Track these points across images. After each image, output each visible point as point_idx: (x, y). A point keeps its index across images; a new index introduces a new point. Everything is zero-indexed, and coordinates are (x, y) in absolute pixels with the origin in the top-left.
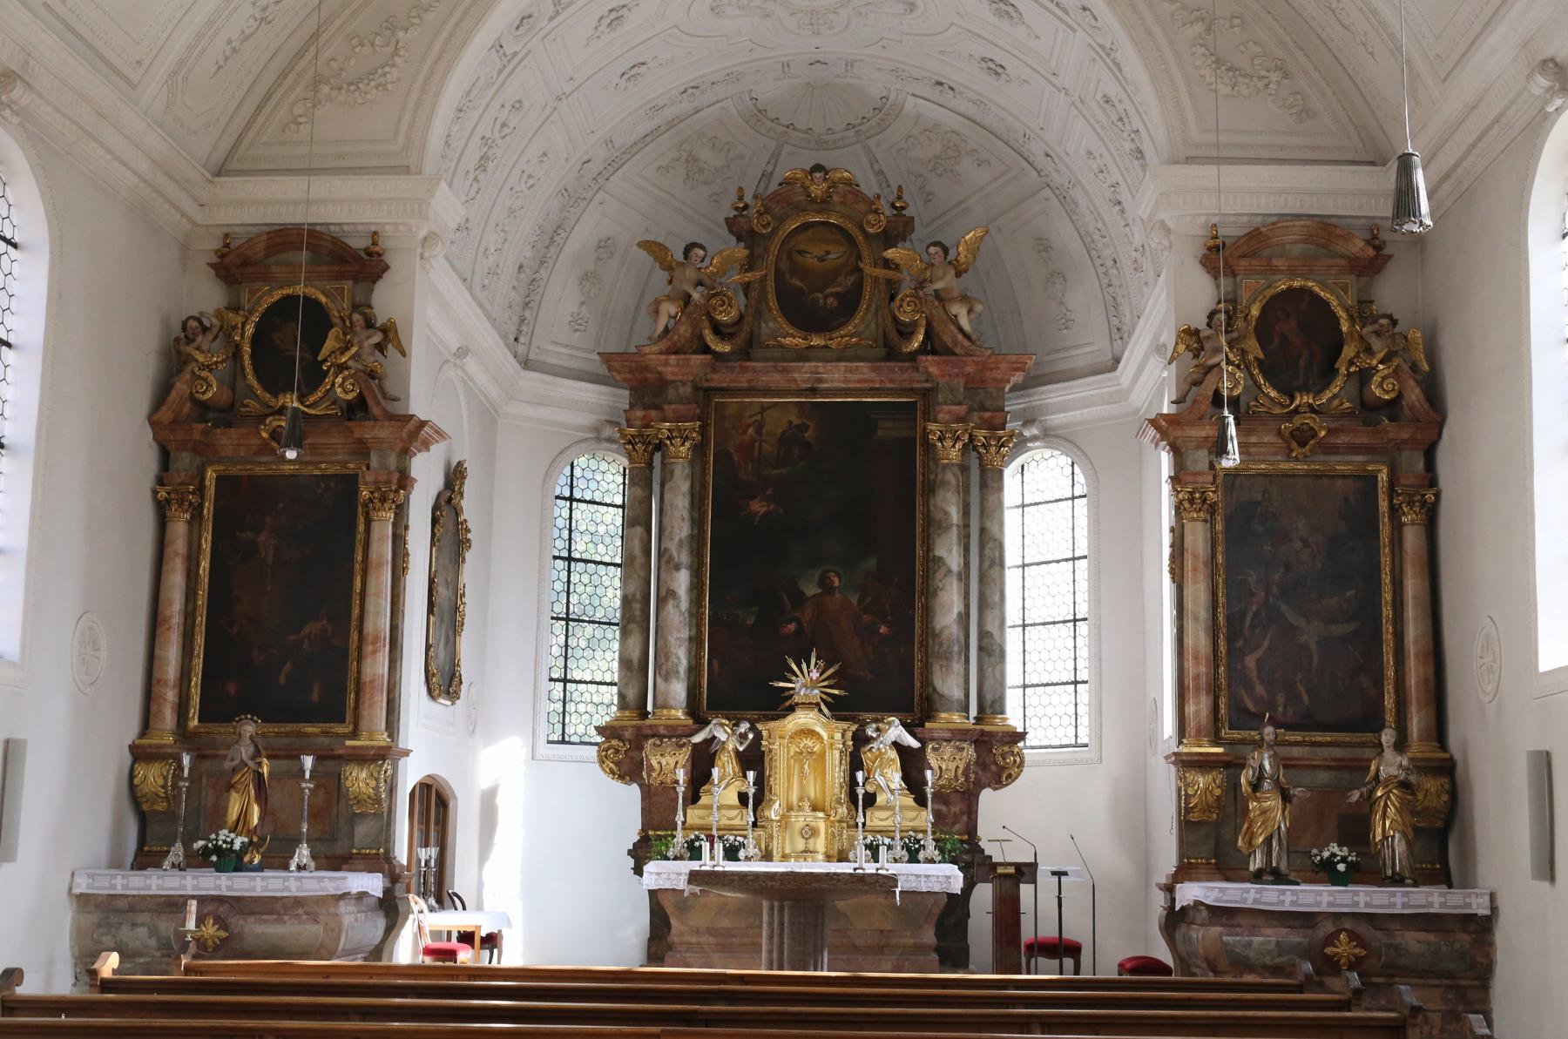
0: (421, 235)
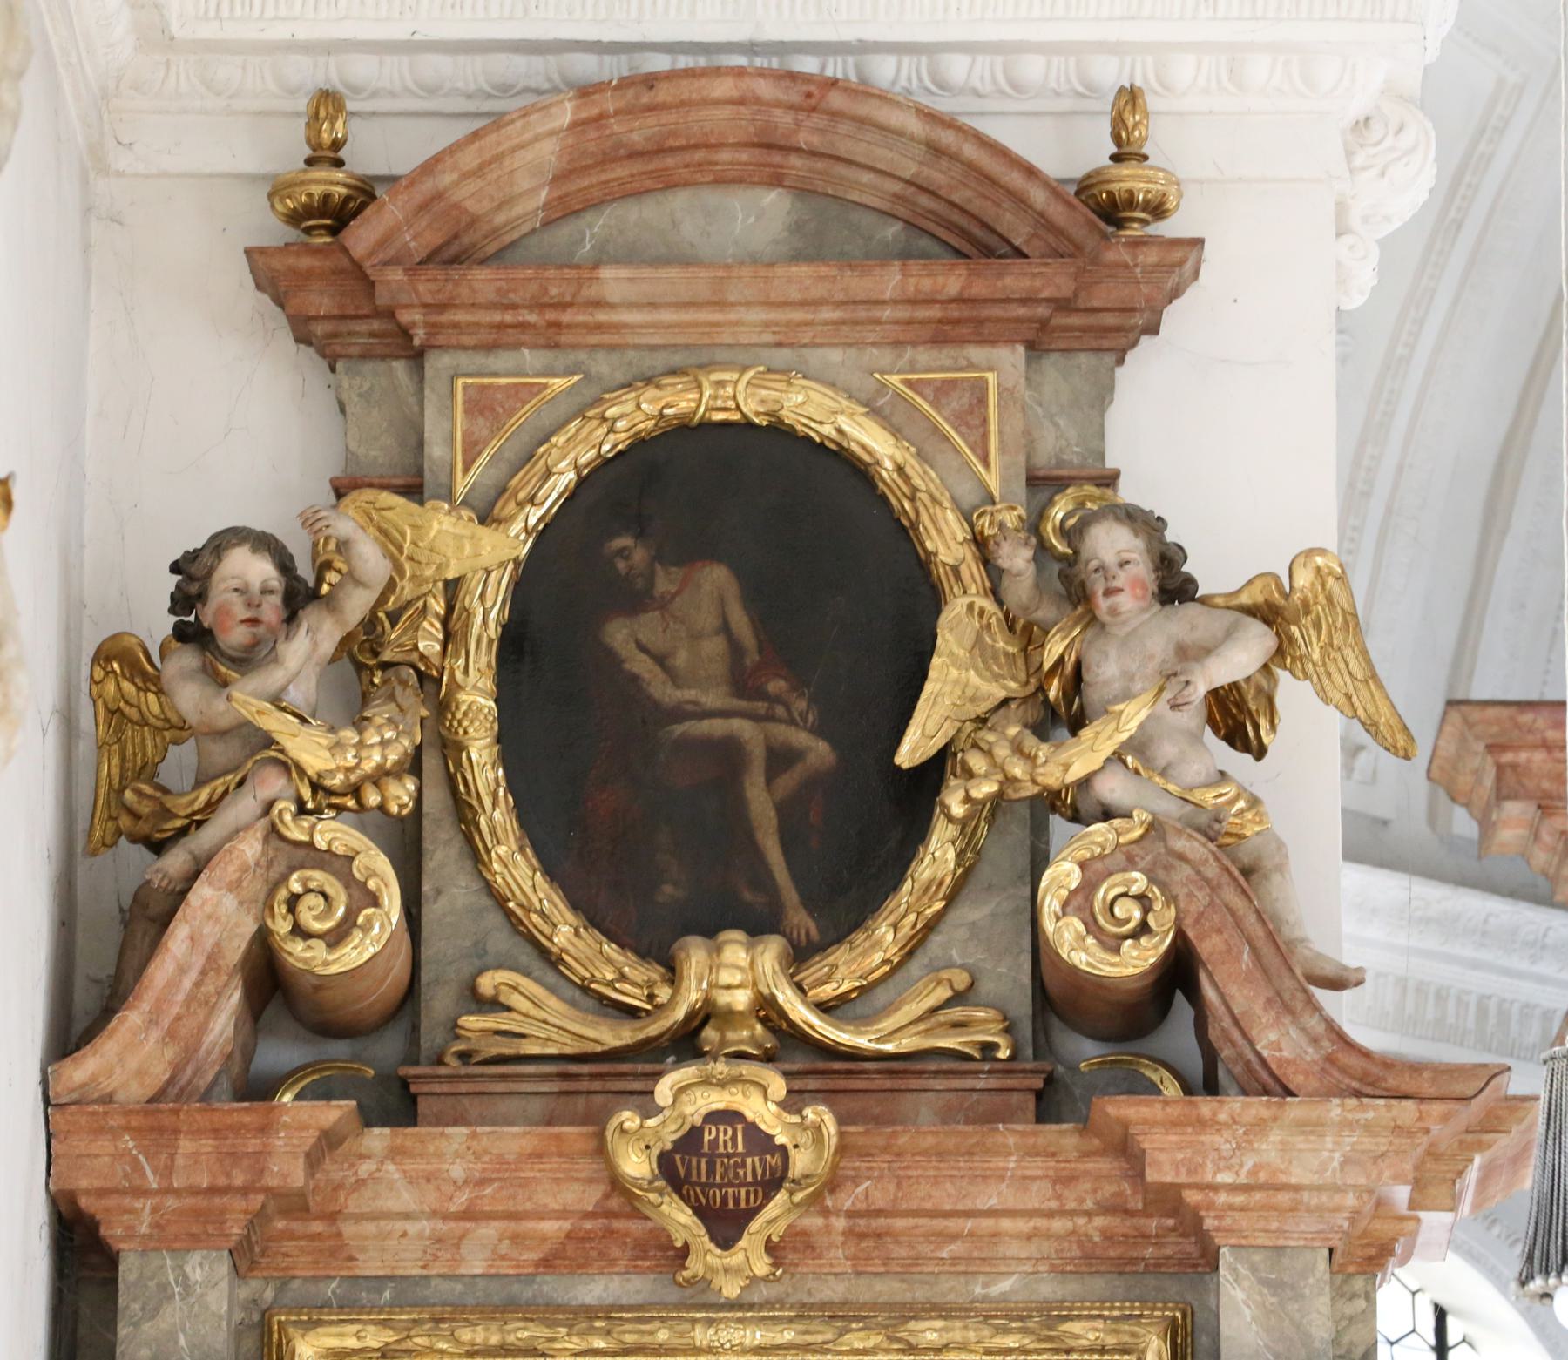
0: (1356, 107)
